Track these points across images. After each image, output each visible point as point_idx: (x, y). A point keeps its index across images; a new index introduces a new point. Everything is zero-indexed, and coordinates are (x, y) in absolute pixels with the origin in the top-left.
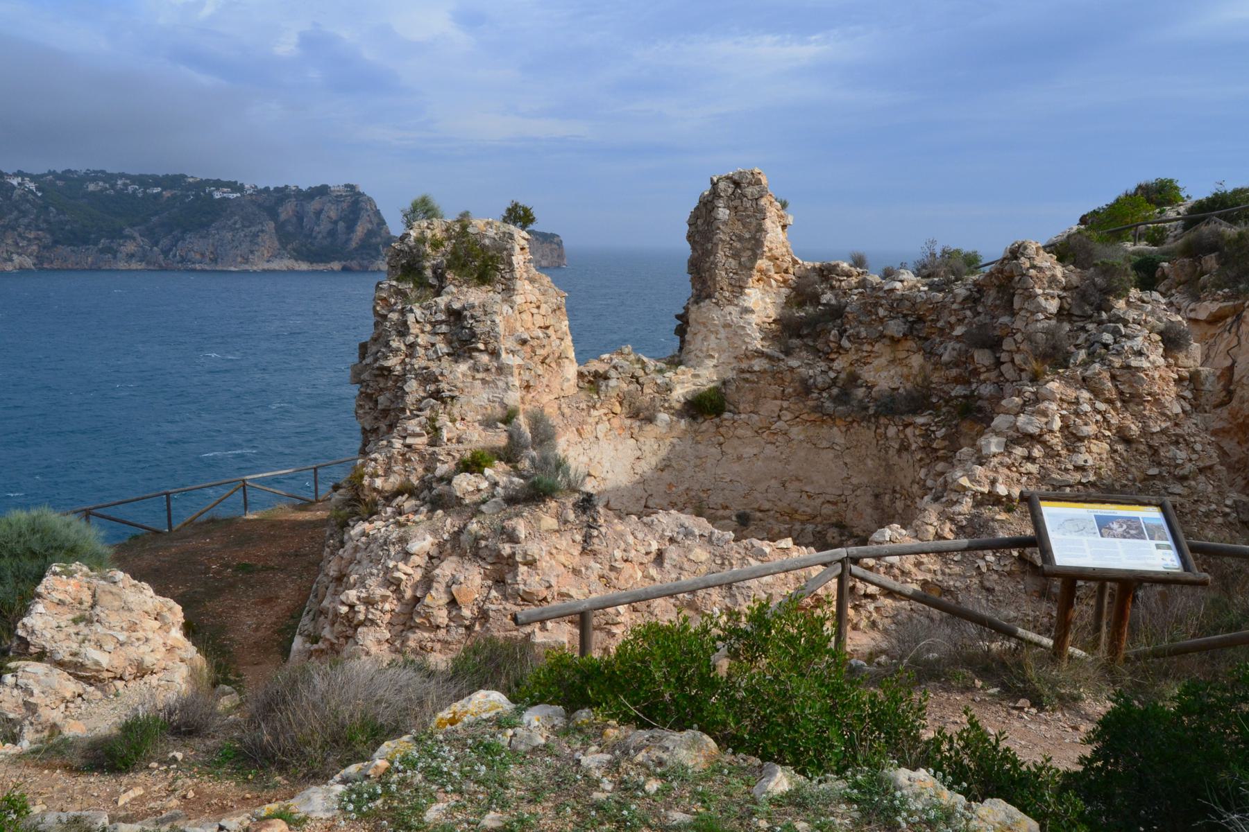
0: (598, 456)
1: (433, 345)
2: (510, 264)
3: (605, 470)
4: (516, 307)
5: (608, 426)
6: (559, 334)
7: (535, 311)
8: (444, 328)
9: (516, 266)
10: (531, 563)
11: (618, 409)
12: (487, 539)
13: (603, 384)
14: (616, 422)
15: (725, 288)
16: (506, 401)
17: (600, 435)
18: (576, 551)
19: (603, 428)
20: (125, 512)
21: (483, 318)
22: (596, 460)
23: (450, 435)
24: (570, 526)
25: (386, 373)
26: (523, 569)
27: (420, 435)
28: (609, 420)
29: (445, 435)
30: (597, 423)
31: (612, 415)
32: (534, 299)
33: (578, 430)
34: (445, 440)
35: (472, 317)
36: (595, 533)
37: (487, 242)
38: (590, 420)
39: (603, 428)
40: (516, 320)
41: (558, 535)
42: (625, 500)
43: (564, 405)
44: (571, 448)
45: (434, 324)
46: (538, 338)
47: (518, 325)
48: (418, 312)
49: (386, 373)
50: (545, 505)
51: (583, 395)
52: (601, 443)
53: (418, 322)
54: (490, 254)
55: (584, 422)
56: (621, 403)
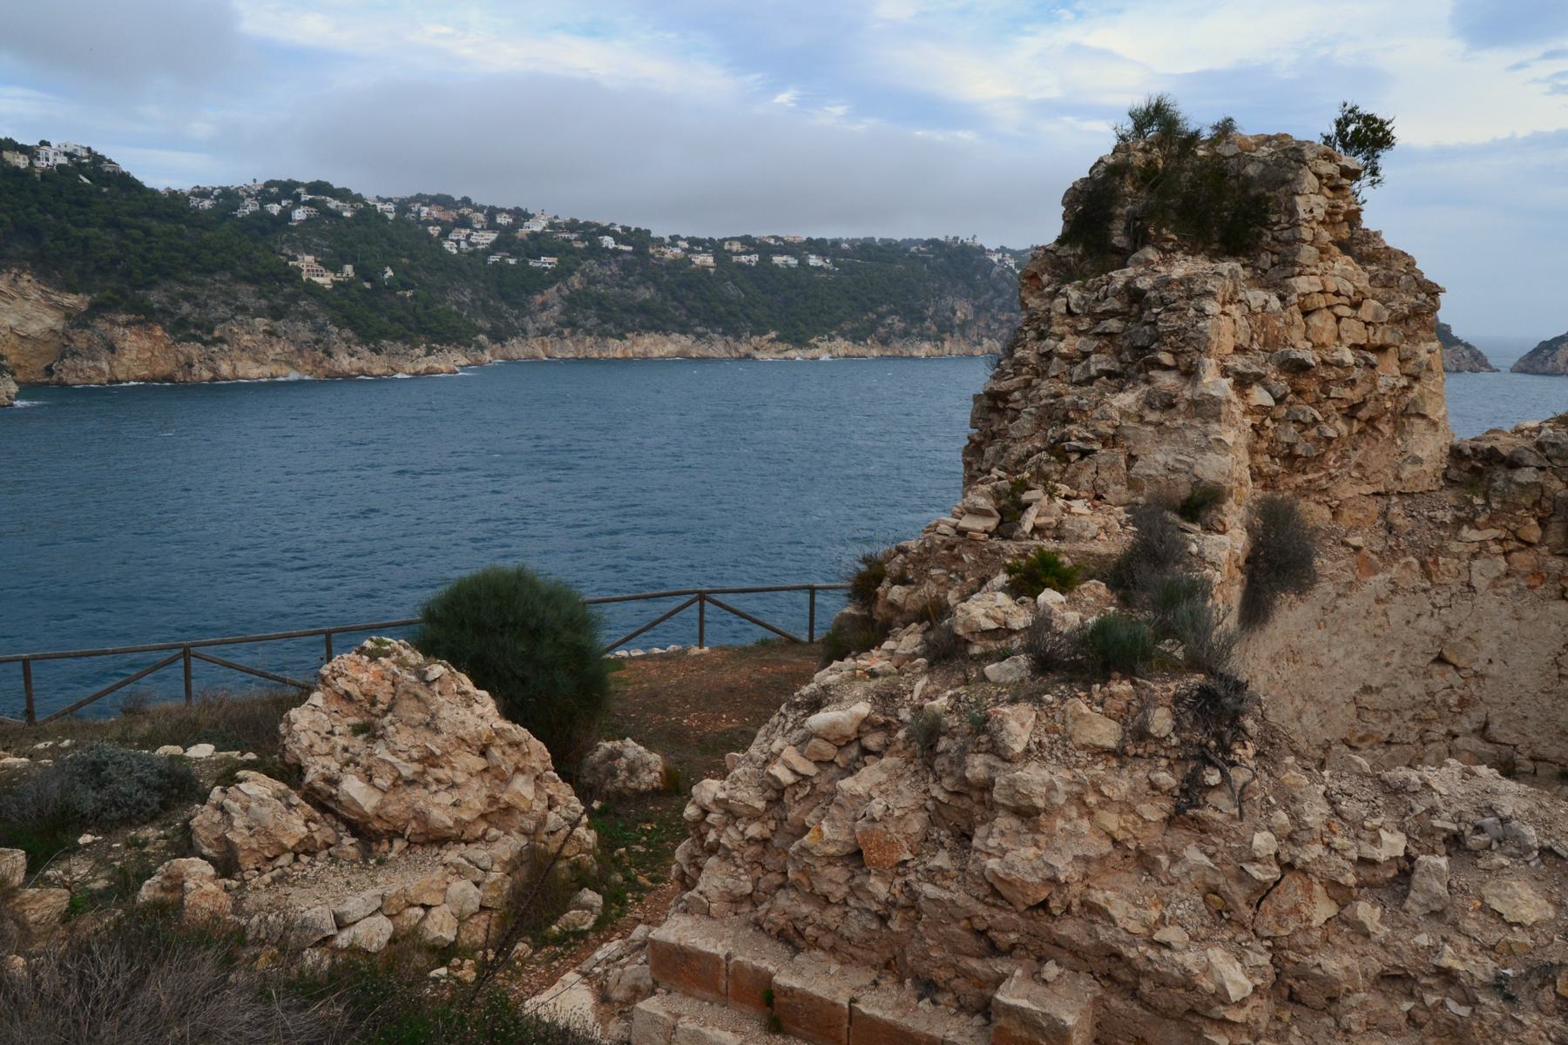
0: (1470, 625)
1: (1086, 355)
2: (1292, 212)
3: (1483, 656)
4: (1294, 298)
5: (1502, 564)
6: (1410, 367)
7: (1345, 311)
8: (1113, 325)
9: (1302, 215)
10: (1027, 814)
11: (1533, 532)
12: (953, 736)
13: (1500, 477)
14: (1524, 560)
16: (1198, 470)
17: (1479, 582)
18: (1153, 812)
19: (1484, 571)
20: (749, 604)
21: (1181, 303)
22: (1463, 631)
23: (1043, 520)
24: (1152, 748)
25: (1001, 405)
26: (1004, 822)
27: (985, 514)
28: (1506, 554)
29: (1029, 520)
30: (1474, 556)
31: (1513, 545)
32: (1348, 288)
33: (1423, 564)
34: (1027, 527)
35: (1162, 301)
36: (1213, 778)
37: (1251, 170)
38: (1455, 547)
39: (1484, 571)
40: (1290, 325)
41: (1114, 763)
42: (1530, 727)
43: (1396, 510)
44: (1398, 598)
45: (1098, 318)
46: (1340, 364)
47: (1296, 335)
48: (1074, 295)
49: (1001, 405)
50: (1104, 683)
51: (1449, 497)
52: (1479, 599)
53: (1070, 312)
54: (1252, 193)
55: (1441, 550)
56: (1542, 523)
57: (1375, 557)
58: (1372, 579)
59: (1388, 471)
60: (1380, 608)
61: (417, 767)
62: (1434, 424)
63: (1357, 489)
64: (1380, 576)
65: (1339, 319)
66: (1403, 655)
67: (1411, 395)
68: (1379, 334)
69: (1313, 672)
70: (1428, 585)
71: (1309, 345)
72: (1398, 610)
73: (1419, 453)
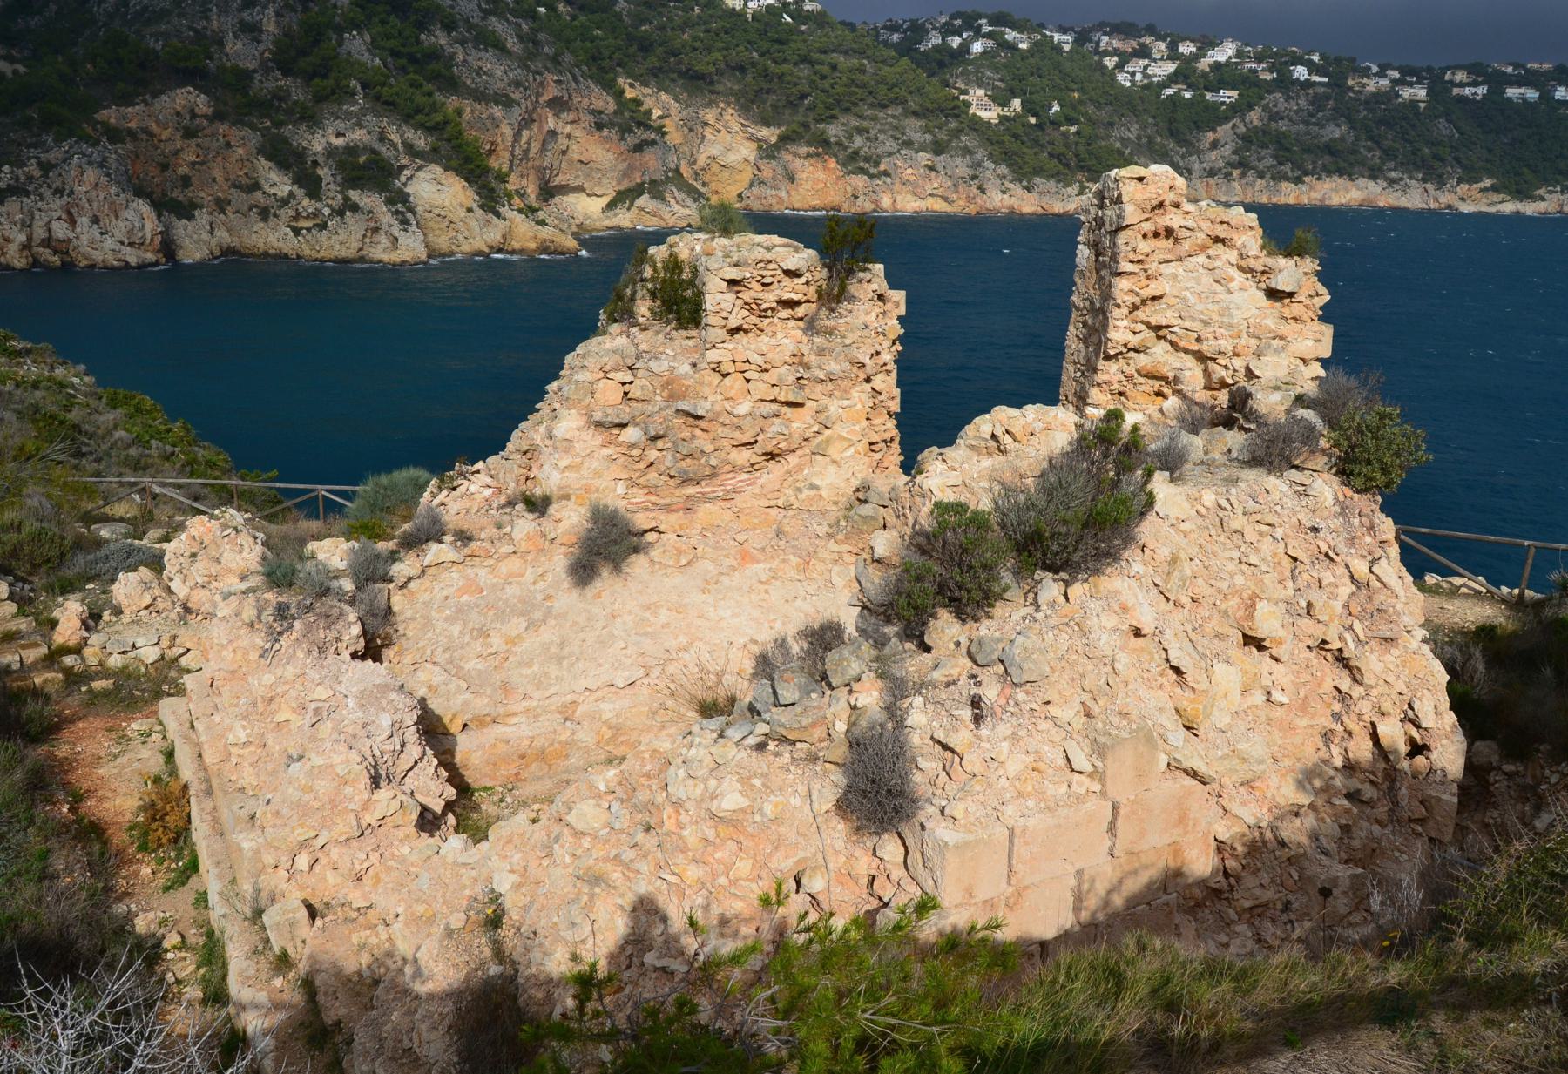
6: (822, 418)
15: (1070, 398)
44: (778, 583)
57: (755, 552)
58: (756, 566)
59: (789, 492)
60: (763, 587)
61: (206, 579)
62: (834, 462)
63: (756, 503)
64: (762, 566)
65: (748, 381)
66: (784, 624)
67: (820, 438)
68: (783, 393)
69: (699, 622)
70: (801, 577)
71: (720, 397)
72: (776, 593)
73: (817, 482)
